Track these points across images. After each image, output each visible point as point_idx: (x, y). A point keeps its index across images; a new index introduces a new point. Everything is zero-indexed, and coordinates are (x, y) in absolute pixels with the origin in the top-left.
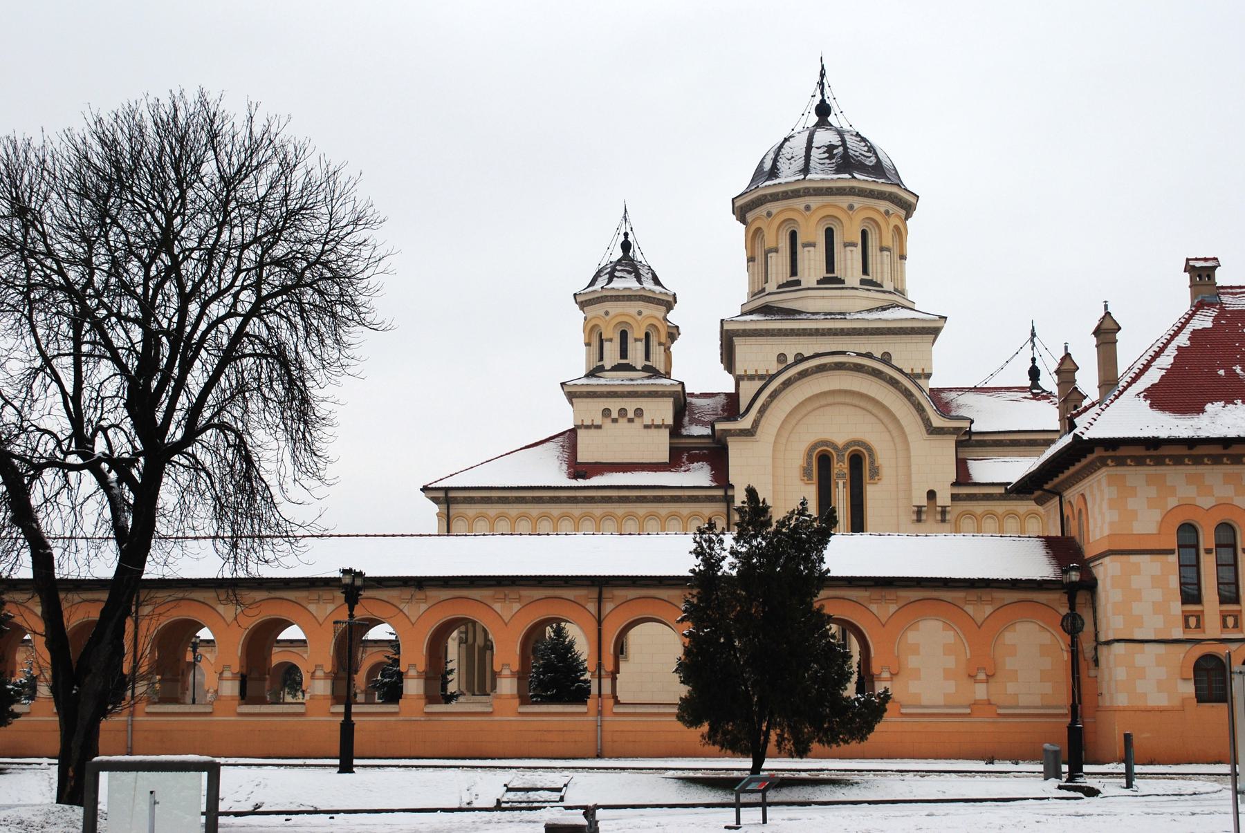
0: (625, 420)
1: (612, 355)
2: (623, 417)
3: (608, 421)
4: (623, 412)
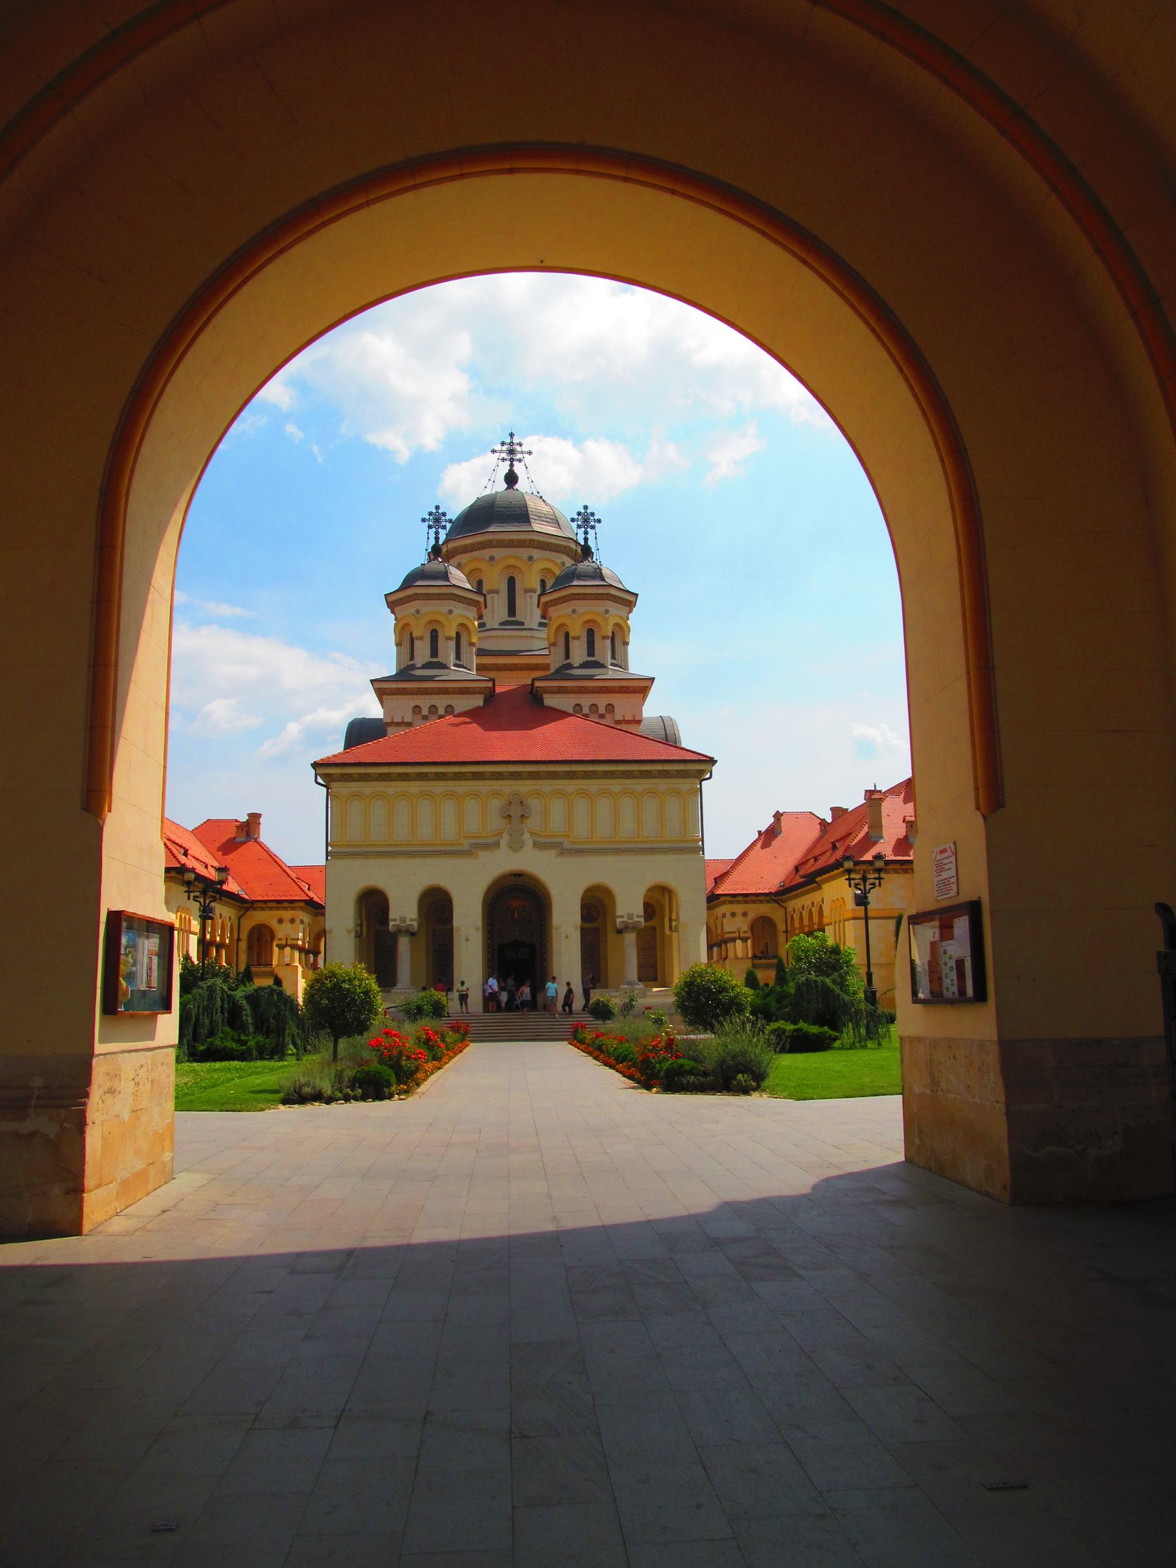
0: (436, 717)
1: (423, 653)
2: (434, 714)
3: (419, 717)
4: (433, 709)
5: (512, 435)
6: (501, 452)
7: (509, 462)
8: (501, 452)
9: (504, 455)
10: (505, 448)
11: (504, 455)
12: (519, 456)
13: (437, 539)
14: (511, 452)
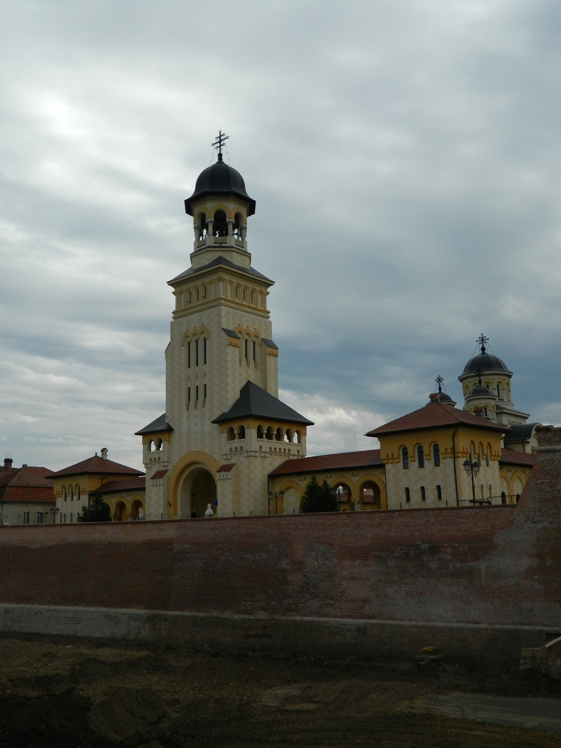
5: (482, 334)
6: (479, 341)
7: (482, 344)
8: (479, 341)
9: (480, 342)
10: (480, 339)
11: (480, 342)
12: (485, 341)
13: (440, 385)
14: (483, 340)
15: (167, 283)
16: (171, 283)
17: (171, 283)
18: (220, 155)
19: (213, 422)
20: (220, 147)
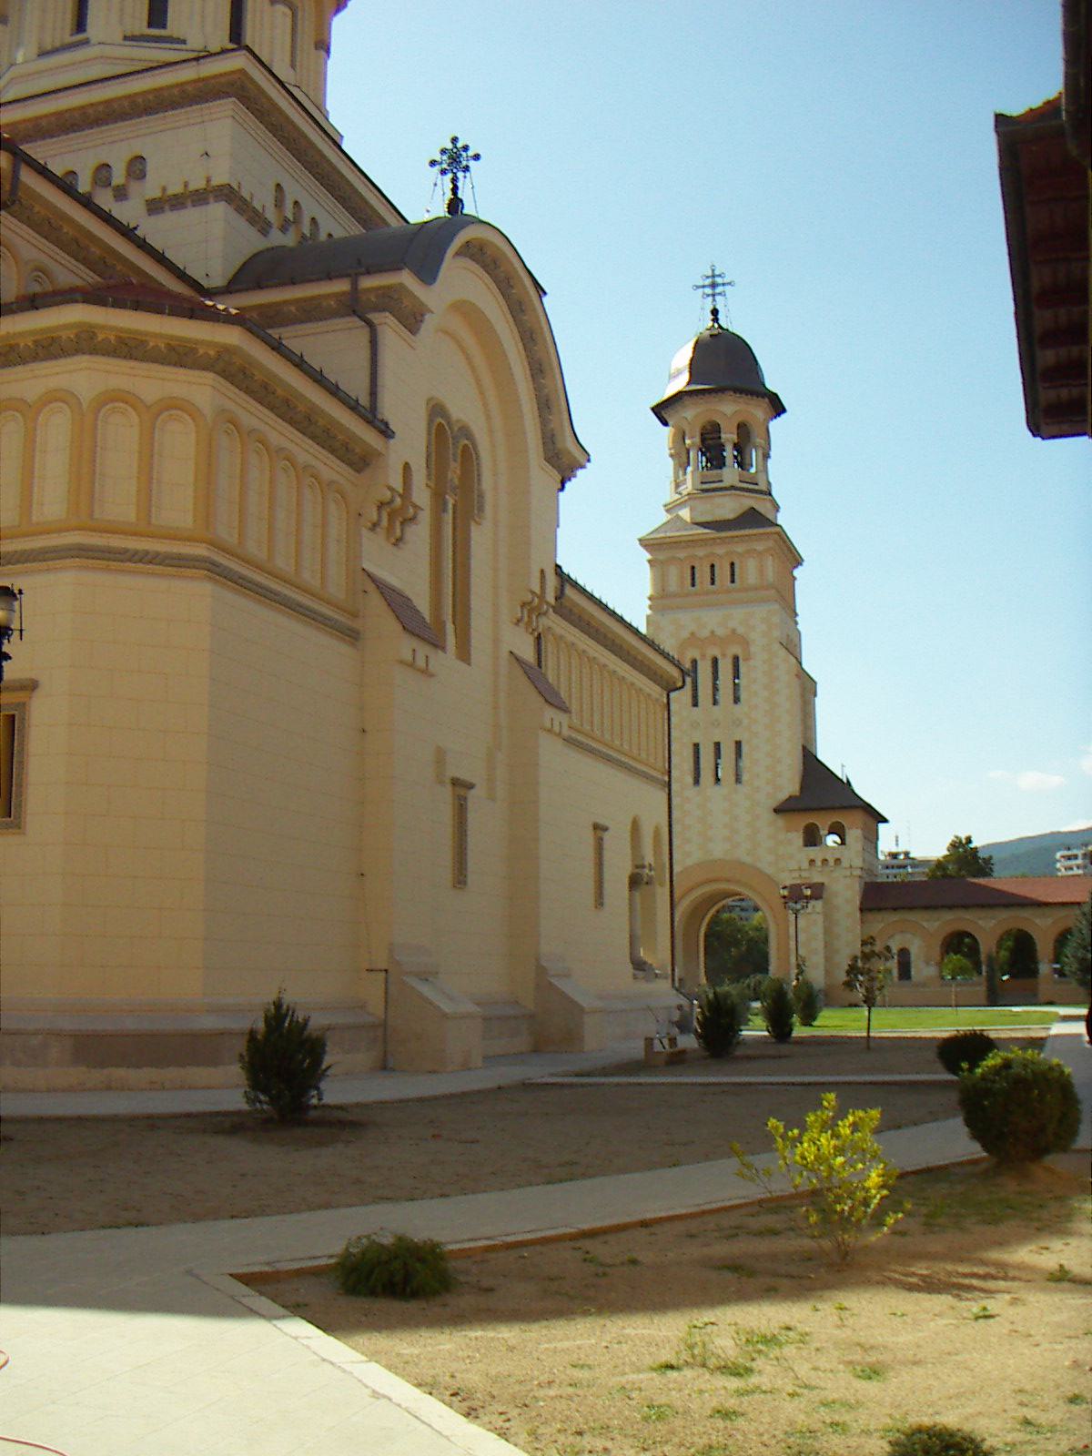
15: (638, 542)
16: (646, 543)
17: (646, 543)
18: (715, 312)
19: (776, 811)
20: (714, 295)
